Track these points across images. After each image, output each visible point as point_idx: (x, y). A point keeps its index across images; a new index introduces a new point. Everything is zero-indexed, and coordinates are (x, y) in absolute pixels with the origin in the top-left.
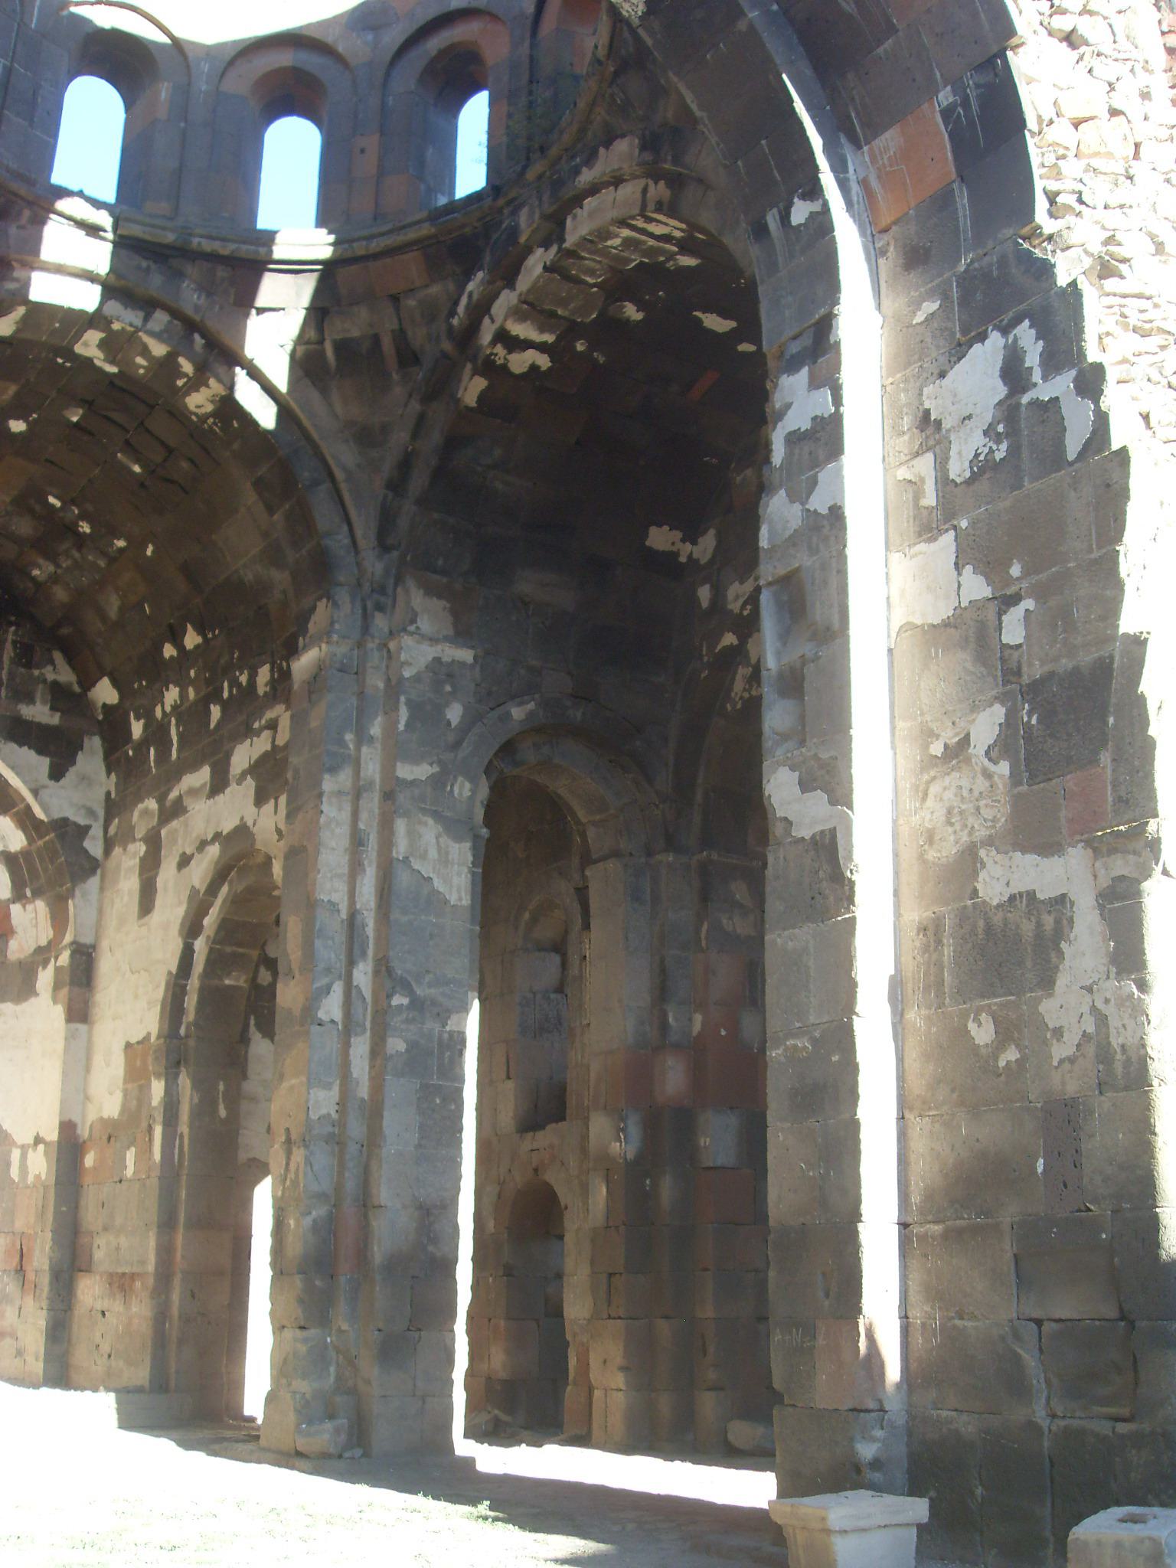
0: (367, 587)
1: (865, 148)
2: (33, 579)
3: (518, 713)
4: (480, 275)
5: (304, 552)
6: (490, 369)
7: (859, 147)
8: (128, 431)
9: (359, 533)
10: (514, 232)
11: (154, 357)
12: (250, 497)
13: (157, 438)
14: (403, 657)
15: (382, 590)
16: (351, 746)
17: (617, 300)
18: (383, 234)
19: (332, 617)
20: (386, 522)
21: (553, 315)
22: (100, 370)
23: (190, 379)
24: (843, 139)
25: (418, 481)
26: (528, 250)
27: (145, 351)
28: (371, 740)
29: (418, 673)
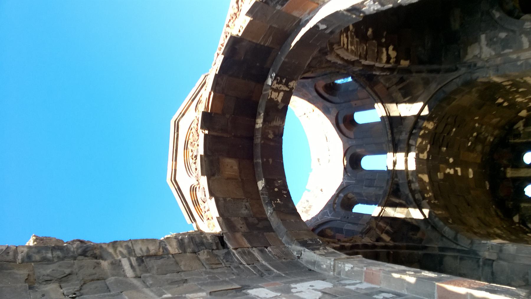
1: (300, 18)
2: (494, 140)
3: (497, 15)
4: (374, 73)
6: (397, 61)
7: (301, 19)
8: (444, 136)
10: (360, 70)
11: (422, 141)
13: (444, 129)
14: (488, 56)
15: (470, 66)
16: (522, 62)
18: (373, 97)
21: (378, 52)
22: (430, 148)
24: (301, 23)
25: (435, 67)
26: (364, 65)
27: (421, 143)
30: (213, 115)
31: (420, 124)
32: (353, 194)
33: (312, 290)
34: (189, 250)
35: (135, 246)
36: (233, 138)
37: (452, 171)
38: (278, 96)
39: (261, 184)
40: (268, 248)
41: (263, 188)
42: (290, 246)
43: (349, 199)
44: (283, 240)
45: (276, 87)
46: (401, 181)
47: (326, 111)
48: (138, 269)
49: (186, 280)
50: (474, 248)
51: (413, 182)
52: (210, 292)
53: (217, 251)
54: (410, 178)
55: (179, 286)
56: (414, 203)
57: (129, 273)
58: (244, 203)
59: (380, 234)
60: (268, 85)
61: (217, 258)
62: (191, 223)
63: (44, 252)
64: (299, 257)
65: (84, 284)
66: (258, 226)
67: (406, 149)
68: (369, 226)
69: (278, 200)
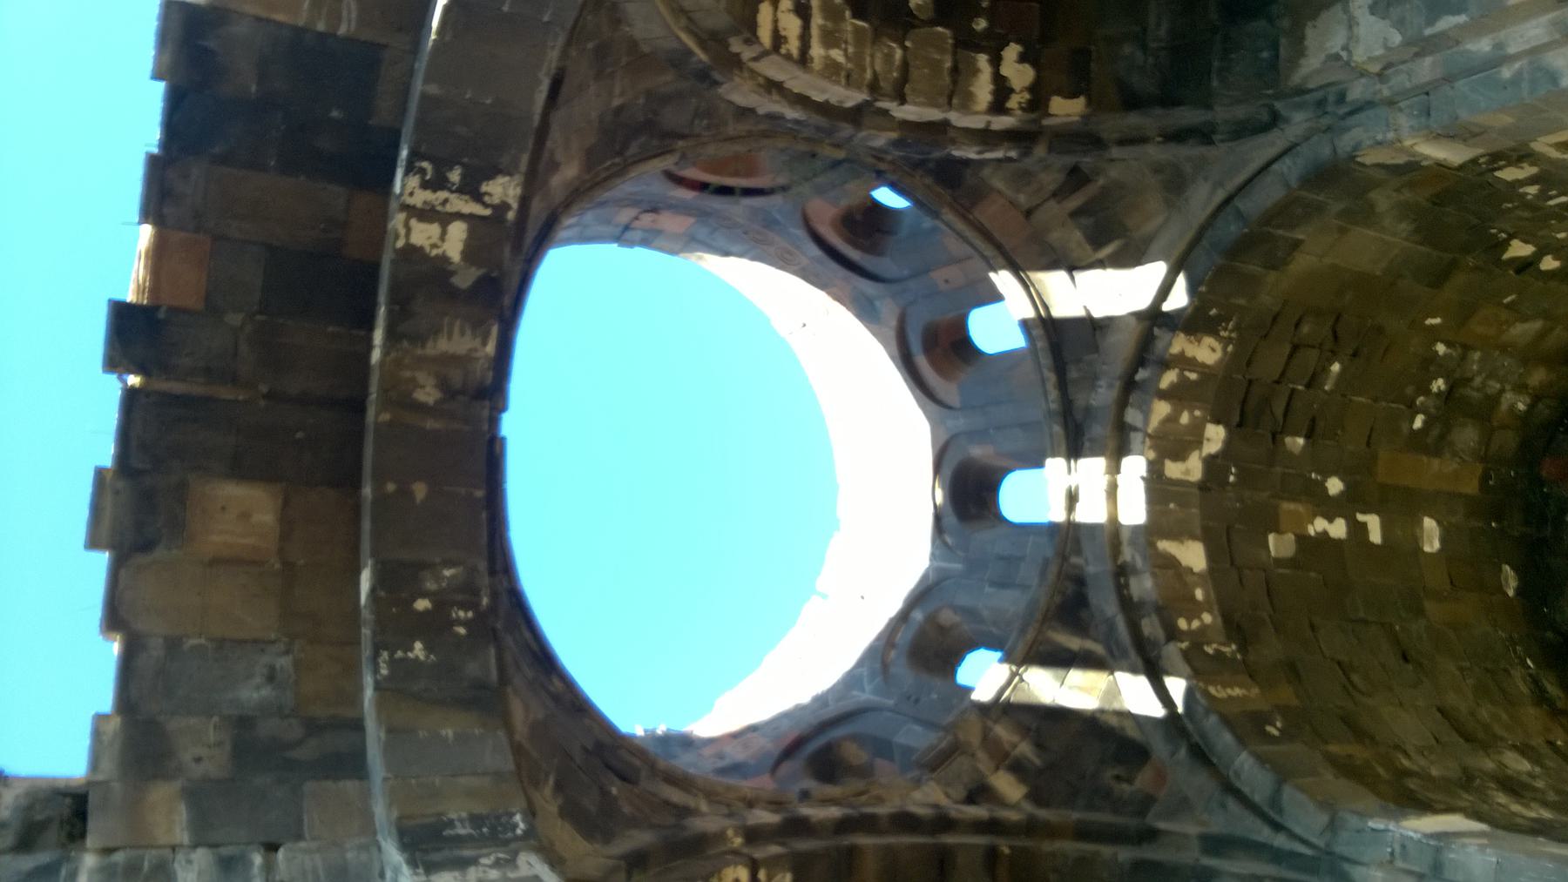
0: (1325, 121)
2: (1531, 407)
4: (956, 153)
5: (1320, 198)
6: (1038, 101)
8: (1293, 390)
9: (1272, 152)
10: (897, 144)
12: (1302, 262)
13: (1287, 364)
14: (1379, 52)
17: (915, 17)
19: (1371, 146)
20: (1245, 130)
21: (955, 70)
23: (1182, 370)
25: (1188, 116)
26: (905, 125)
27: (1171, 419)
28: (1499, 46)
29: (1394, 26)
30: (161, 315)
31: (1159, 345)
32: (956, 613)
36: (262, 403)
37: (1338, 529)
38: (443, 237)
43: (943, 630)
45: (425, 202)
46: (1095, 567)
47: (865, 311)
50: (1339, 849)
51: (1135, 572)
54: (1127, 554)
56: (1133, 654)
58: (265, 659)
66: (296, 754)
67: (1111, 444)
69: (418, 646)
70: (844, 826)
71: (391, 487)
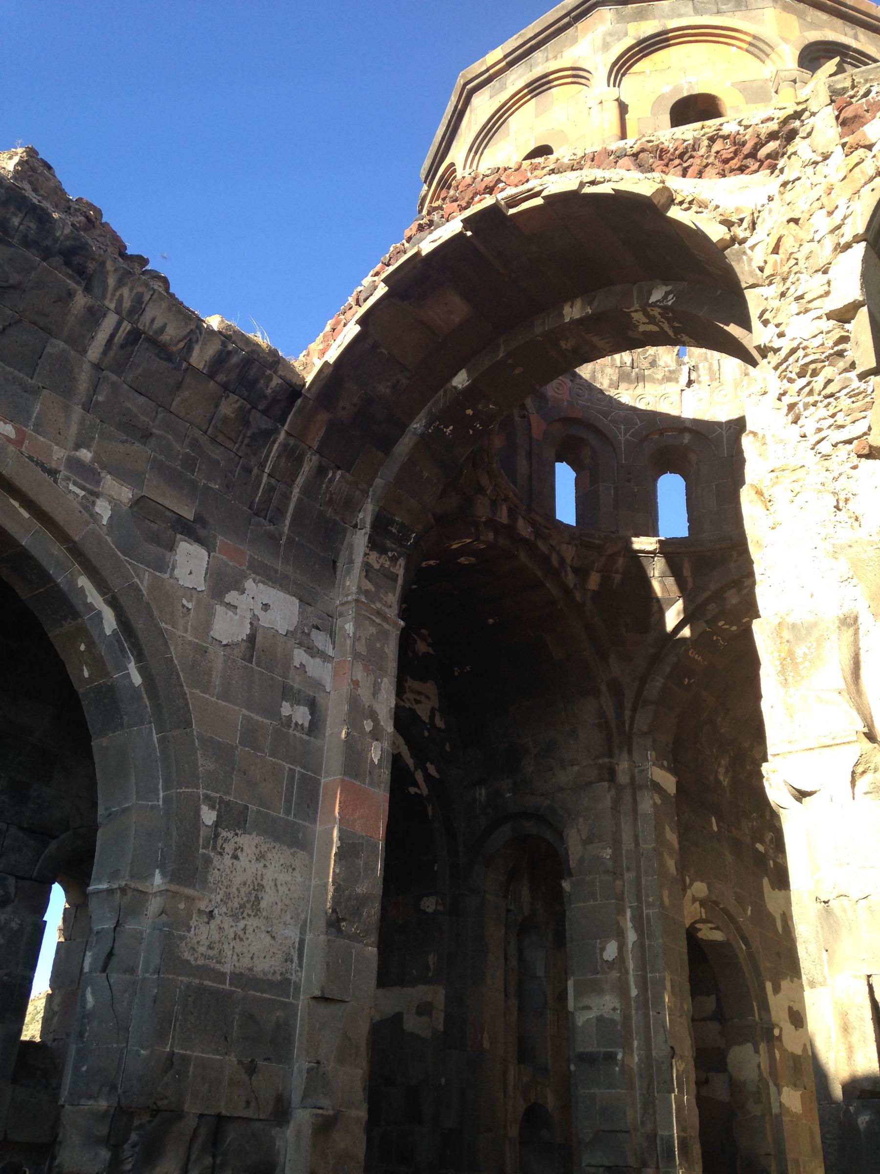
32: (696, 464)
33: (249, 615)
34: (221, 377)
35: (150, 305)
38: (644, 324)
39: (461, 380)
40: (339, 472)
41: (455, 388)
42: (370, 500)
44: (378, 481)
48: (112, 353)
49: (151, 434)
52: (144, 496)
53: (258, 415)
55: (123, 442)
57: (94, 352)
59: (595, 569)
60: (650, 294)
61: (241, 428)
62: (423, 180)
63: (12, 209)
64: (355, 526)
65: (19, 321)
68: (602, 542)
69: (451, 428)
70: (525, 541)
71: (510, 361)
